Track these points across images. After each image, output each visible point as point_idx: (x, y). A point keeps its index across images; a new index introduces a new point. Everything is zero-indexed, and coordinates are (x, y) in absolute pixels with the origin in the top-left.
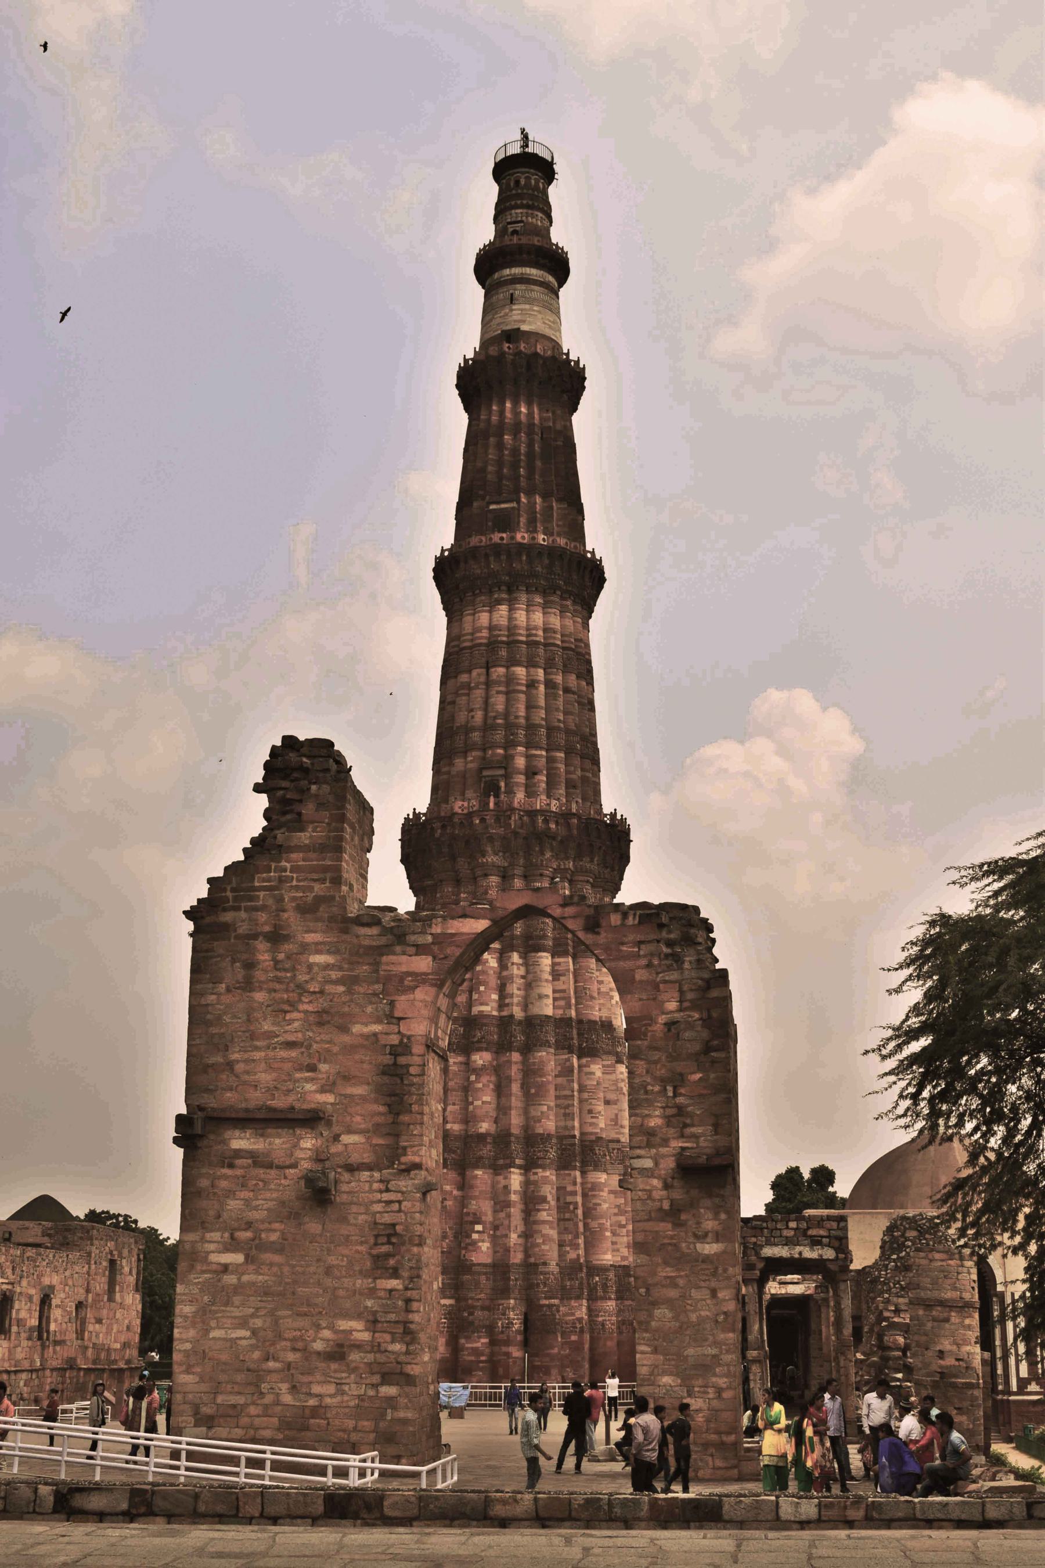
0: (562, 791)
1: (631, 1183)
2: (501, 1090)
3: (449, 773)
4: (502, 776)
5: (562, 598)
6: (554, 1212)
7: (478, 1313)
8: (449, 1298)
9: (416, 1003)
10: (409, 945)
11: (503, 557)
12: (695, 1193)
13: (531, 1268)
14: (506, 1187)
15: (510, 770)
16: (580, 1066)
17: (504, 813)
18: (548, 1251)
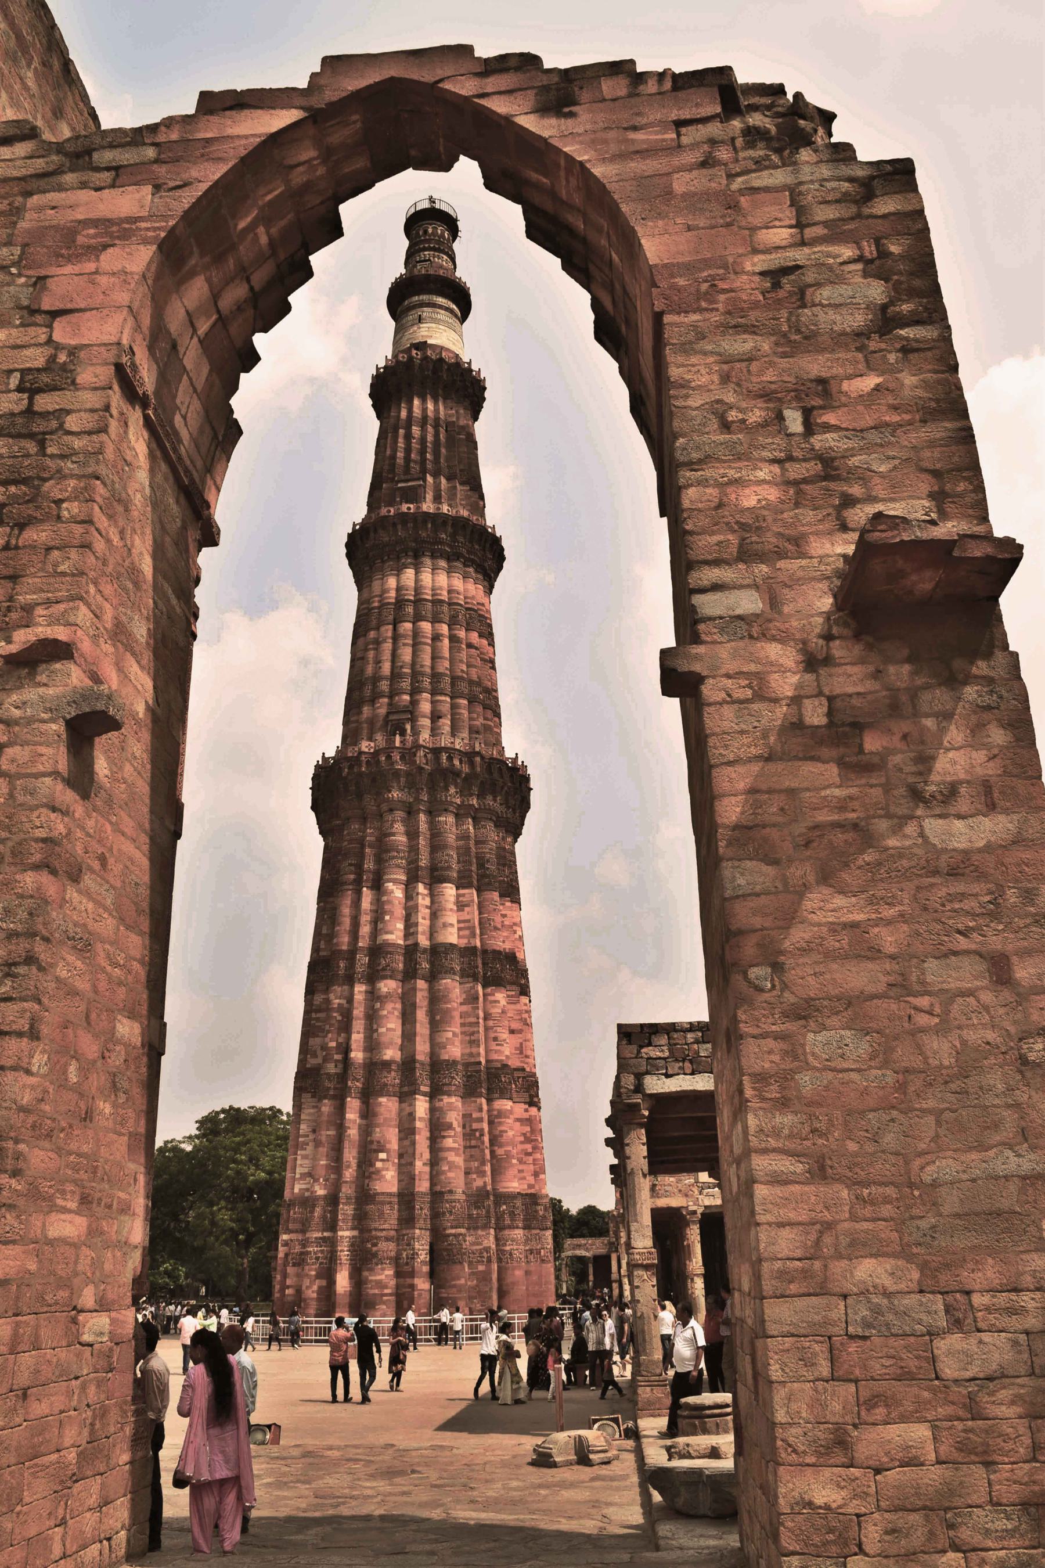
0: (465, 734)
1: (698, 658)
2: (408, 1017)
3: (357, 721)
5: (465, 566)
6: (460, 1140)
7: (383, 1245)
8: (353, 1229)
9: (103, 280)
10: (98, 169)
12: (900, 674)
13: (437, 1196)
16: (484, 995)
17: (409, 754)
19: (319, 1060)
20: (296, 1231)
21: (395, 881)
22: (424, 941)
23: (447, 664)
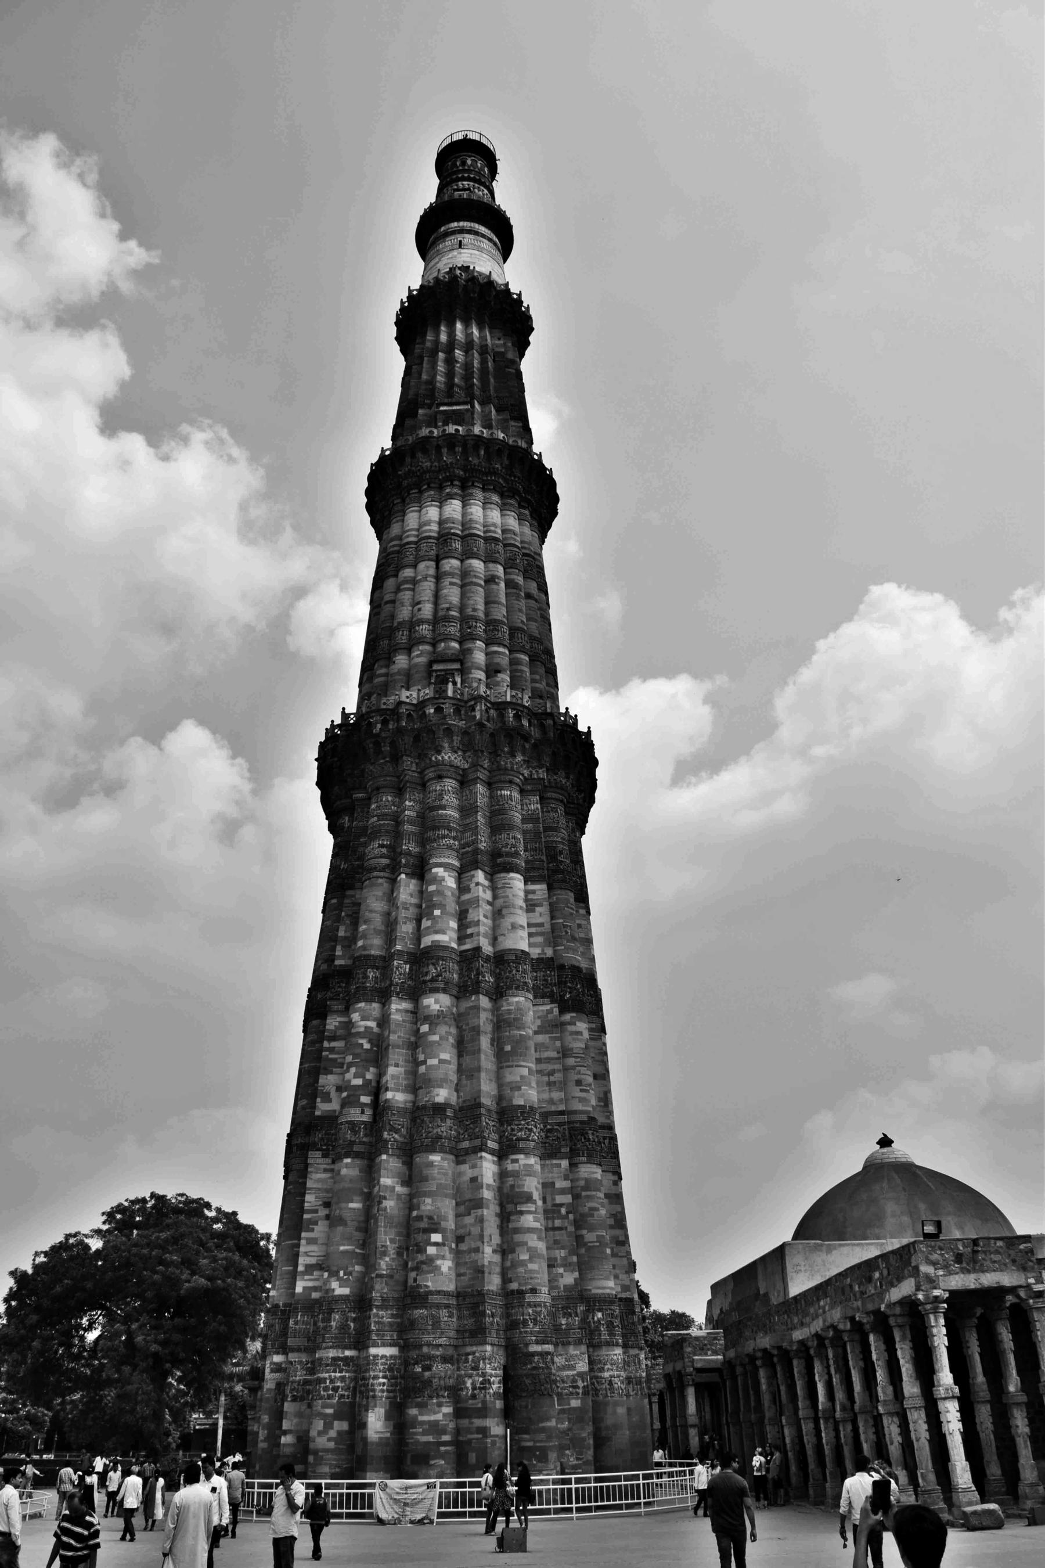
2: (464, 1046)
4: (457, 670)
5: (520, 506)
6: (541, 1216)
7: (438, 1368)
8: (391, 1345)
11: (459, 449)
14: (474, 1180)
15: (469, 664)
18: (537, 1272)
19: (334, 1106)
20: (298, 1350)
21: (446, 866)
22: (487, 949)
23: (504, 611)
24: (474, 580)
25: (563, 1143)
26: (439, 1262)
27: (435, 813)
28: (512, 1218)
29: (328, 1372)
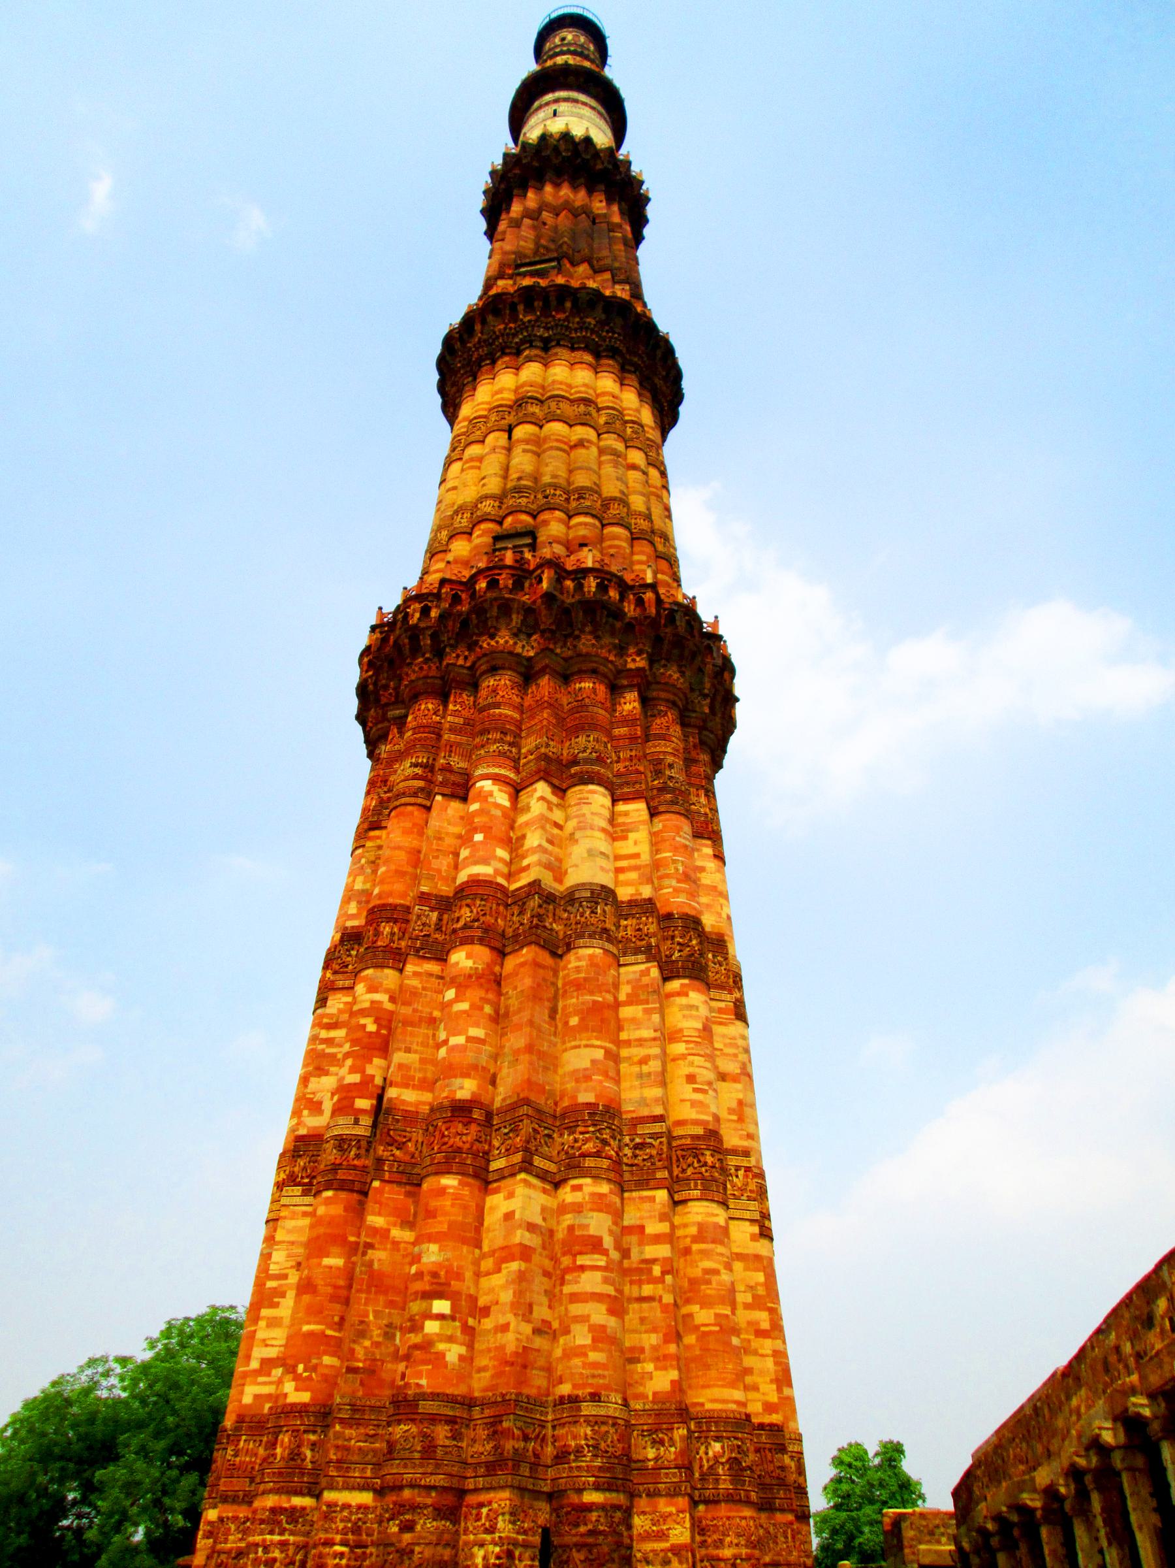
8: (362, 1488)
15: (542, 537)
18: (604, 1366)
21: (496, 778)
22: (548, 881)
24: (555, 444)
25: (659, 1164)
26: (441, 1346)
27: (485, 713)
28: (568, 1277)
29: (262, 1533)
